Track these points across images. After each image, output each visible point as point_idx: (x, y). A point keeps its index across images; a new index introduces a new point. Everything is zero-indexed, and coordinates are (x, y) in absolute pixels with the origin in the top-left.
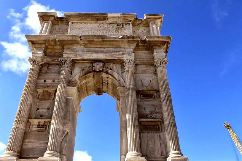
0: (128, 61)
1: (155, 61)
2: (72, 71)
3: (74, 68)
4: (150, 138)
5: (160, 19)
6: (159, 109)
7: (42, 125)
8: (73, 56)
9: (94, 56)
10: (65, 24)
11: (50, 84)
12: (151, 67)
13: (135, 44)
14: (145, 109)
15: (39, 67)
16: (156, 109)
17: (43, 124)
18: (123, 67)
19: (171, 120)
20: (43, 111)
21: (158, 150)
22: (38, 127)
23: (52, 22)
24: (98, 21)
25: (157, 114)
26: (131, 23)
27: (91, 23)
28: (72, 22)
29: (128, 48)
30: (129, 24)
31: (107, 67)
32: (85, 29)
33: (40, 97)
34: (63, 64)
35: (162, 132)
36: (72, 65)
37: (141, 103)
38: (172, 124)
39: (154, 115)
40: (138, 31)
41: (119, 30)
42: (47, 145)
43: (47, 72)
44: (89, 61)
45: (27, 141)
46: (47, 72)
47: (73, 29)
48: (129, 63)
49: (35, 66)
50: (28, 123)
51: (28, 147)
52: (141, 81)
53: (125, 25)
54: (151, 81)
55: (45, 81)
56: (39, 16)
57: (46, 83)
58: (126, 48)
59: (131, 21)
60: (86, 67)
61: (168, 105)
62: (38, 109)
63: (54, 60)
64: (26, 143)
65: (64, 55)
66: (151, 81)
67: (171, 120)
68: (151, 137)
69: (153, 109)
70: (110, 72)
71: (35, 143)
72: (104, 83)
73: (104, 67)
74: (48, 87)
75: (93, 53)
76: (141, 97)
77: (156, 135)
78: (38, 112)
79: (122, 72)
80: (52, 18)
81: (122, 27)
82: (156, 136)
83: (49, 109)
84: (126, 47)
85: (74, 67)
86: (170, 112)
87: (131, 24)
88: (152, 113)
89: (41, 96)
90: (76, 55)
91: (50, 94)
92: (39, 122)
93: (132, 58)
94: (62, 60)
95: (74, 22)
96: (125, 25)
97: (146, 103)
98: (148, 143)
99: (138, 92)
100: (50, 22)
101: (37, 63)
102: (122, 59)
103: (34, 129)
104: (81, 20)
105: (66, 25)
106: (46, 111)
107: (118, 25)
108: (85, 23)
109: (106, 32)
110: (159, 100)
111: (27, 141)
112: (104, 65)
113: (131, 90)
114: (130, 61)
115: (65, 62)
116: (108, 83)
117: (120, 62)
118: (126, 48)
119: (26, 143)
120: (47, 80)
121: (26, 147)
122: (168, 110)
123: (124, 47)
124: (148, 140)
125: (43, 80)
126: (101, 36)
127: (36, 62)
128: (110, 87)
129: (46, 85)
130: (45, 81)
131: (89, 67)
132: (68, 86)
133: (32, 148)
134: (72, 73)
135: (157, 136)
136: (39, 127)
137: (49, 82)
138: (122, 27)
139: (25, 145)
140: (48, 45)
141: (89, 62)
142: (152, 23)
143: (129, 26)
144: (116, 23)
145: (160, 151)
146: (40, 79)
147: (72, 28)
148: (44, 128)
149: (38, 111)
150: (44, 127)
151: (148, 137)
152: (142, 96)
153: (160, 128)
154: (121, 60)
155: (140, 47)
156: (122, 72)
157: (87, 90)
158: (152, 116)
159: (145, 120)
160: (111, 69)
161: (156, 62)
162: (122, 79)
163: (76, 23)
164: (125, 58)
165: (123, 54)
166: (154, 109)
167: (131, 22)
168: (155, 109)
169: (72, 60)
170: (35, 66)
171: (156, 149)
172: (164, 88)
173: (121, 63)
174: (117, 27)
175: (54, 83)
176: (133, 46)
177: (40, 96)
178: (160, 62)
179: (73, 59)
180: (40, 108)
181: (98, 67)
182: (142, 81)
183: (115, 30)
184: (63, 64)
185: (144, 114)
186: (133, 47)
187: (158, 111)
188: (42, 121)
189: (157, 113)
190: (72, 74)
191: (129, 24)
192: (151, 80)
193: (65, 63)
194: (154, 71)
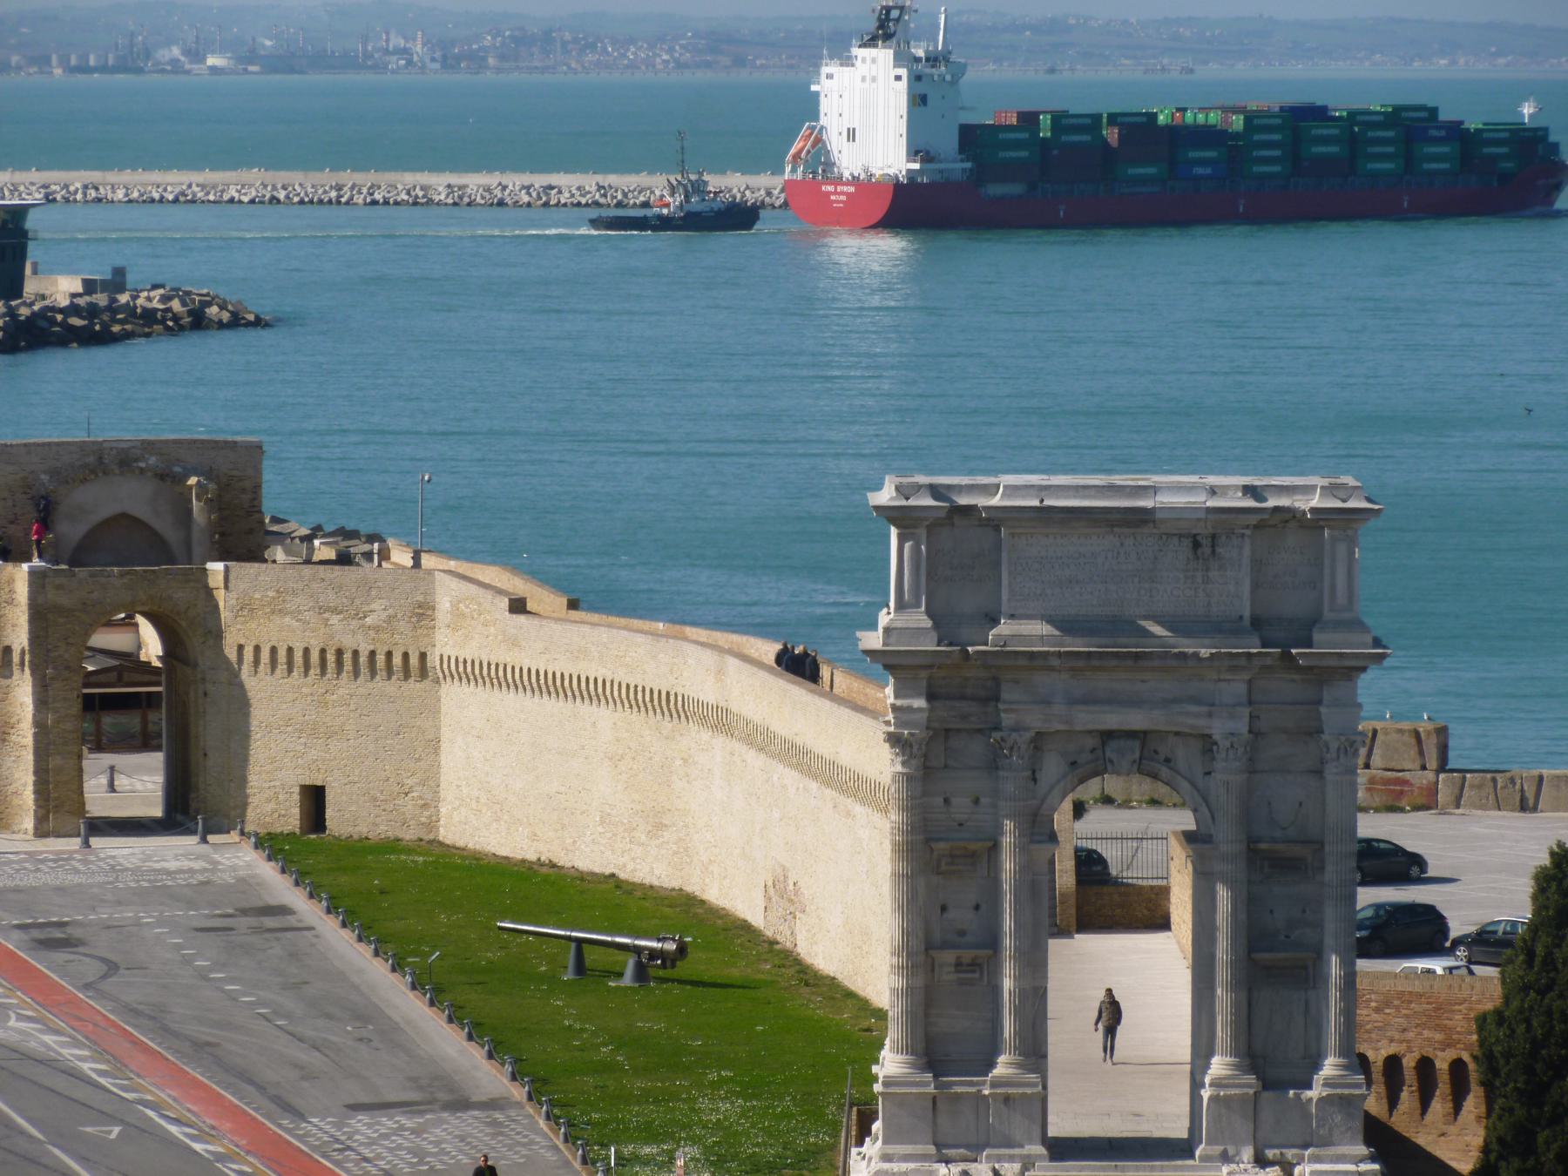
7: (969, 965)
8: (1035, 720)
9: (1112, 719)
10: (976, 523)
14: (1271, 912)
20: (962, 916)
22: (957, 971)
24: (1115, 529)
26: (1248, 532)
29: (1229, 680)
30: (1243, 535)
31: (1156, 752)
33: (944, 868)
35: (1314, 987)
36: (1036, 748)
43: (946, 766)
46: (946, 766)
48: (1231, 752)
50: (932, 967)
52: (1269, 804)
53: (1224, 538)
54: (1301, 804)
55: (946, 801)
58: (1225, 680)
62: (944, 909)
63: (964, 717)
66: (1301, 804)
74: (961, 825)
81: (1214, 552)
83: (977, 907)
84: (1222, 677)
91: (973, 856)
92: (958, 958)
93: (1242, 726)
94: (1003, 739)
96: (1224, 538)
102: (1206, 731)
103: (948, 976)
107: (1196, 545)
109: (1147, 586)
114: (1232, 746)
115: (1011, 749)
118: (1225, 680)
120: (955, 801)
123: (1216, 677)
125: (941, 800)
127: (911, 746)
130: (946, 801)
131: (1092, 752)
132: (1032, 842)
134: (1038, 776)
137: (961, 805)
138: (1214, 552)
144: (1187, 536)
148: (977, 975)
149: (945, 915)
150: (974, 972)
158: (1292, 938)
159: (1266, 956)
160: (1168, 760)
162: (1204, 805)
163: (1021, 534)
164: (1218, 728)
165: (1210, 715)
168: (1304, 911)
170: (914, 762)
177: (943, 863)
183: (1181, 576)
188: (968, 955)
190: (1035, 780)
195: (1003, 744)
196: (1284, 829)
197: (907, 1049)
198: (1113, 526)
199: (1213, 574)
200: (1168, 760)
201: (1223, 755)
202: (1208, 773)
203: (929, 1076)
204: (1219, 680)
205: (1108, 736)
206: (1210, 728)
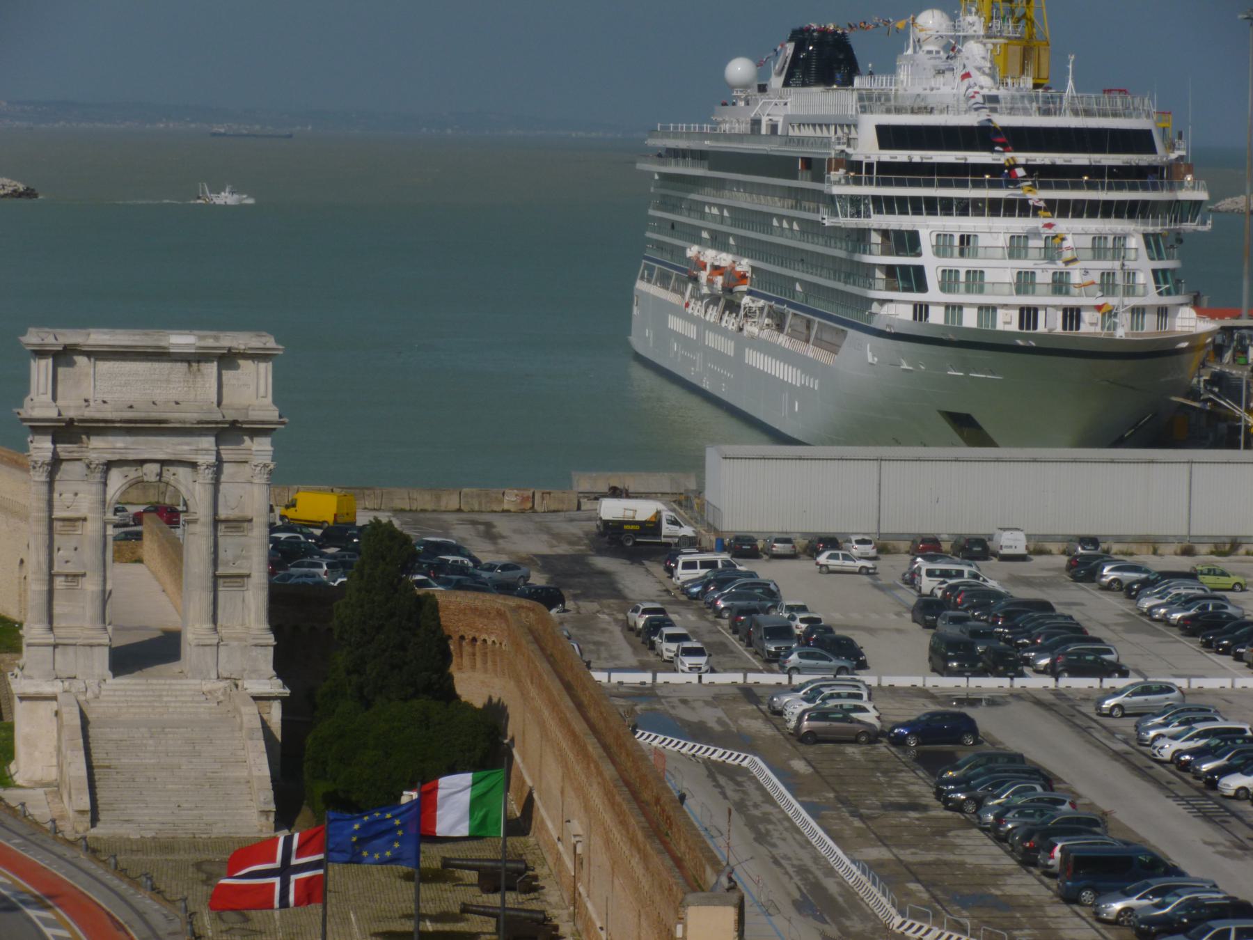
22: (66, 582)
39: (239, 562)
41: (191, 380)
48: (207, 471)
54: (241, 497)
62: (59, 550)
74: (68, 507)
83: (76, 549)
88: (237, 558)
90: (114, 453)
107: (190, 366)
130: (61, 495)
137: (68, 496)
149: (61, 552)
173: (193, 465)
174: (187, 370)
181: (151, 470)
189: (245, 558)
196: (233, 509)
199: (199, 379)
200: (174, 474)
205: (142, 462)
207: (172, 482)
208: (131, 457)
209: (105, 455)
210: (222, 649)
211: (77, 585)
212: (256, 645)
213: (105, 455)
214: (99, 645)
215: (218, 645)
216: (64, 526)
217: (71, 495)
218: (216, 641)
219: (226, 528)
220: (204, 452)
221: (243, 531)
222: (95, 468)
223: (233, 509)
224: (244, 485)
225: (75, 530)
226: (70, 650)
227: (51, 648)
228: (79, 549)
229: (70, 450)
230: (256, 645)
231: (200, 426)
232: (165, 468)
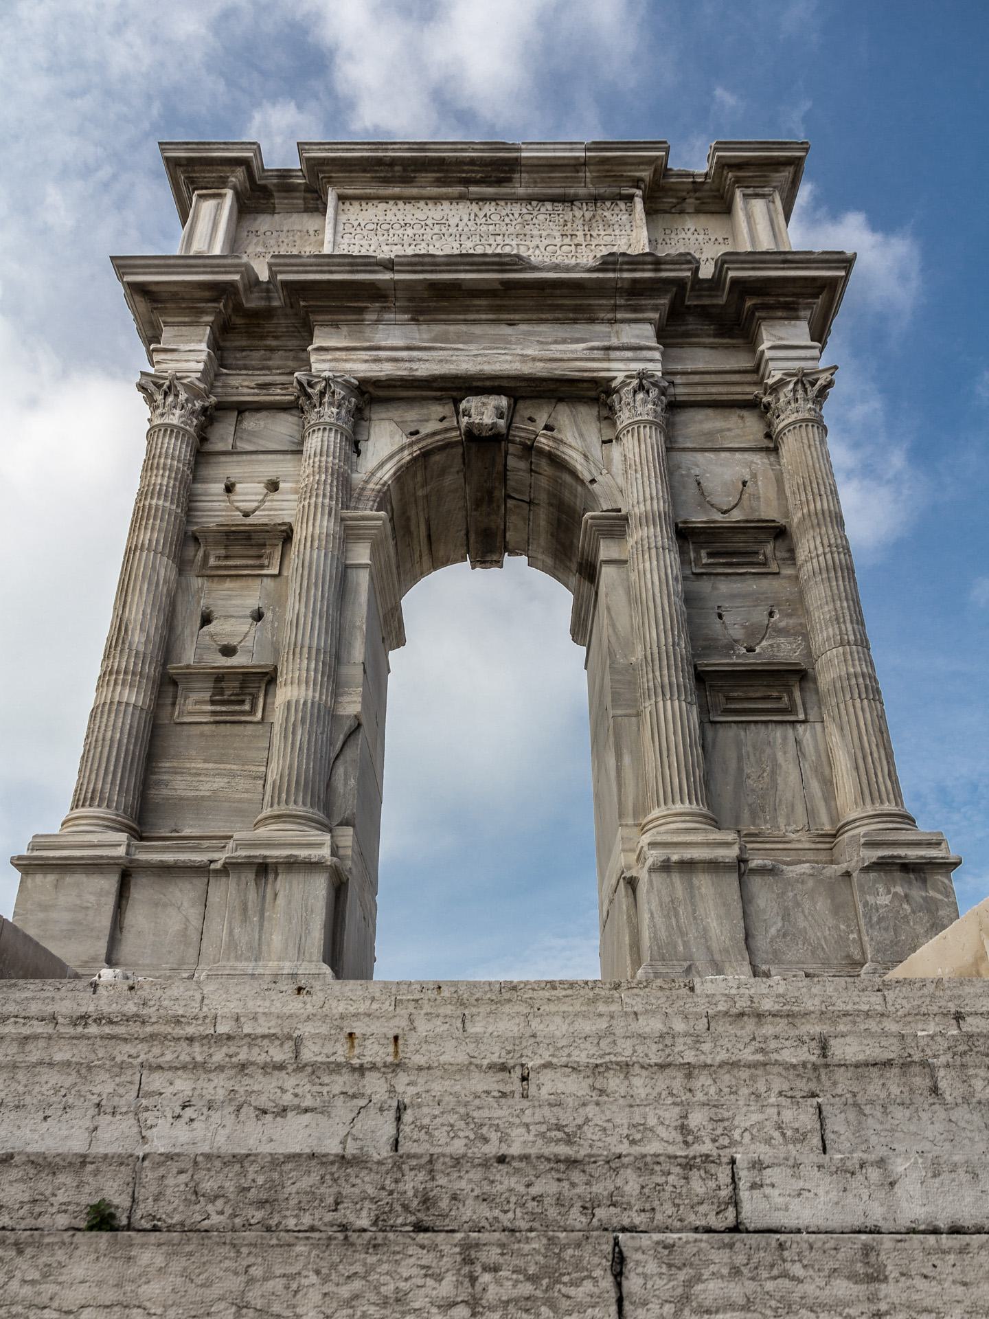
0: (635, 382)
1: (770, 381)
2: (359, 438)
3: (364, 423)
4: (750, 749)
5: (791, 169)
6: (790, 616)
11: (256, 504)
12: (742, 417)
13: (664, 301)
14: (720, 616)
15: (195, 422)
16: (777, 616)
17: (237, 691)
18: (608, 415)
19: (857, 662)
21: (793, 806)
22: (213, 702)
23: (238, 196)
25: (782, 640)
26: (639, 192)
27: (437, 199)
28: (341, 191)
31: (531, 420)
32: (410, 231)
34: (316, 400)
37: (705, 586)
38: (861, 680)
39: (764, 643)
40: (673, 236)
41: (580, 233)
42: (262, 782)
44: (441, 389)
45: (167, 765)
47: (348, 228)
49: (174, 411)
51: (173, 793)
52: (699, 484)
54: (744, 486)
55: (229, 489)
56: (168, 160)
57: (234, 497)
59: (637, 183)
60: (427, 421)
61: (836, 592)
62: (206, 620)
63: (263, 386)
64: (165, 777)
65: (313, 358)
66: (744, 486)
67: (854, 666)
68: (754, 747)
69: (760, 616)
70: (543, 440)
71: (206, 775)
72: (510, 503)
73: (517, 419)
75: (460, 346)
76: (698, 559)
77: (778, 733)
78: (212, 636)
79: (604, 442)
80: (237, 176)
82: (779, 741)
83: (258, 616)
85: (370, 420)
86: (849, 625)
87: (639, 205)
89: (218, 558)
90: (377, 360)
93: (656, 368)
95: (350, 191)
97: (724, 587)
98: (740, 770)
99: (685, 535)
100: (229, 193)
101: (183, 396)
104: (386, 181)
105: (306, 210)
106: (245, 626)
108: (407, 199)
110: (787, 571)
111: (167, 765)
112: (513, 409)
113: (655, 526)
114: (641, 387)
115: (322, 394)
116: (530, 503)
117: (592, 394)
118: (623, 321)
119: (165, 777)
120: (238, 486)
121: (165, 792)
122: (837, 619)
123: (610, 316)
124: (740, 759)
126: (497, 259)
127: (176, 396)
128: (542, 518)
129: (238, 509)
130: (229, 489)
133: (196, 798)
134: (362, 446)
135: (785, 739)
136: (223, 703)
137: (250, 492)
139: (159, 783)
140: (230, 311)
141: (439, 394)
142: (750, 191)
143: (631, 212)
145: (800, 809)
146: (205, 481)
147: (340, 227)
148: (247, 707)
149: (205, 628)
150: (242, 702)
151: (739, 744)
152: (703, 553)
153: (799, 701)
154: (595, 382)
155: (690, 319)
156: (604, 442)
157: (429, 536)
158: (758, 649)
161: (775, 389)
164: (619, 370)
166: (766, 618)
167: (638, 187)
168: (771, 614)
169: (356, 382)
170: (178, 412)
171: (780, 800)
172: (816, 514)
175: (276, 496)
176: (655, 308)
178: (791, 386)
179: (361, 375)
180: (215, 614)
182: (704, 484)
183: (558, 234)
184: (316, 400)
185: (716, 640)
186: (657, 316)
187: (782, 624)
189: (781, 632)
190: (358, 453)
191: (630, 198)
192: (747, 477)
193: (326, 399)
194: (761, 435)
195: (310, 390)
196: (724, 512)
197: (92, 798)
198: (467, 182)
201: (630, 400)
202: (610, 441)
203: (123, 837)
204: (616, 321)
206: (609, 370)
207: (544, 442)
208: (423, 370)
209: (348, 366)
210: (756, 883)
211: (252, 712)
212: (881, 866)
213: (348, 366)
214: (293, 865)
215: (740, 866)
216: (227, 557)
217: (260, 488)
218: (732, 853)
219: (710, 555)
220: (629, 354)
221: (765, 564)
222: (322, 394)
223: (724, 512)
224: (748, 456)
225: (262, 567)
226: (183, 894)
227: (109, 884)
228: (268, 615)
229: (269, 379)
230: (881, 866)
231: (611, 275)
232: (525, 410)
